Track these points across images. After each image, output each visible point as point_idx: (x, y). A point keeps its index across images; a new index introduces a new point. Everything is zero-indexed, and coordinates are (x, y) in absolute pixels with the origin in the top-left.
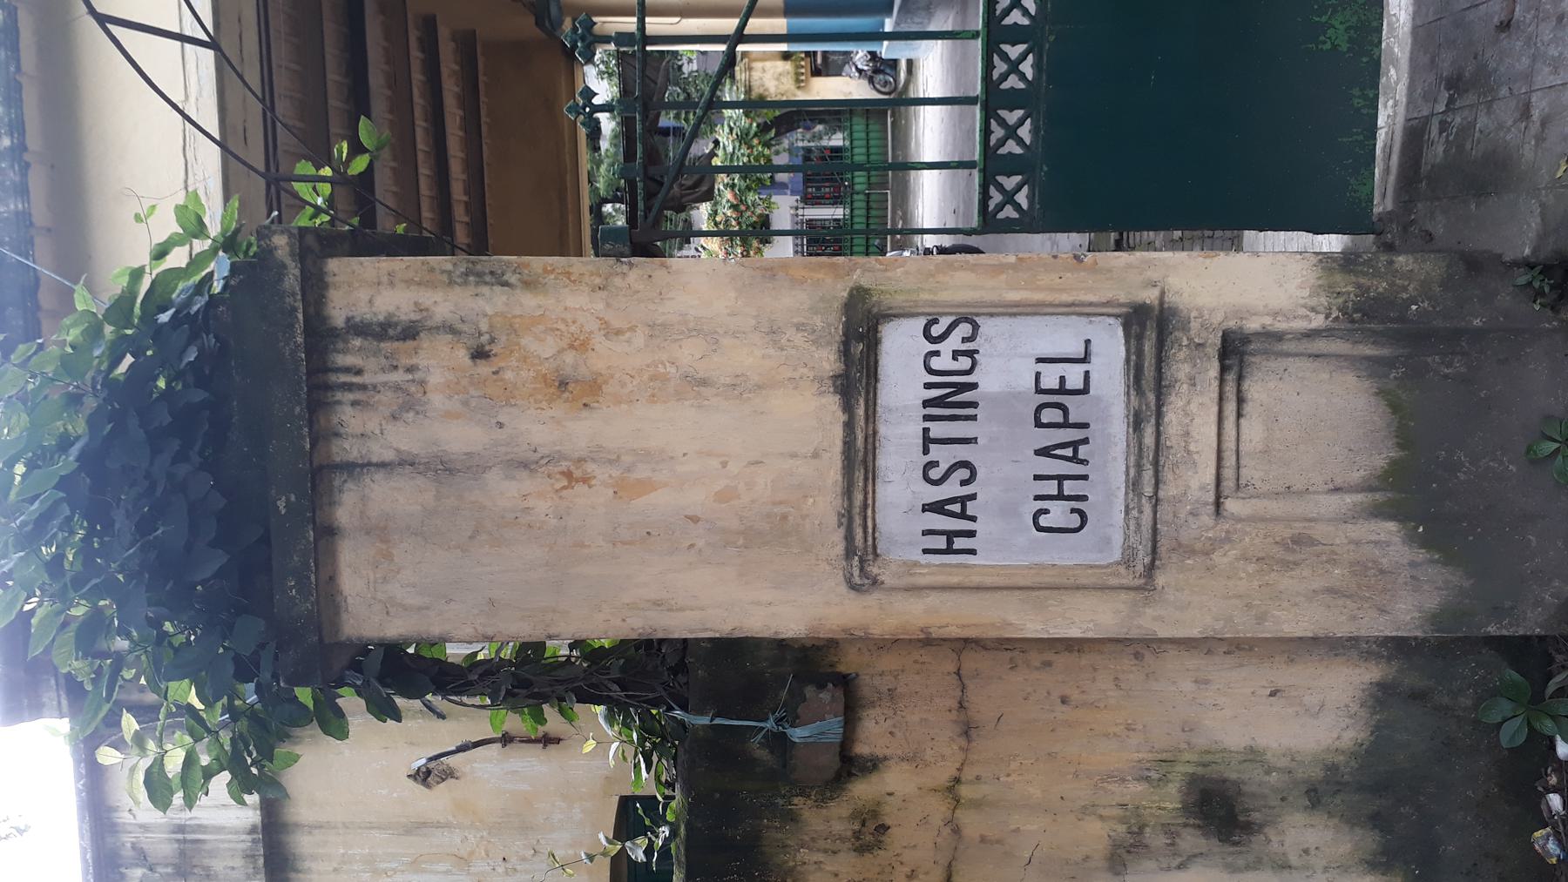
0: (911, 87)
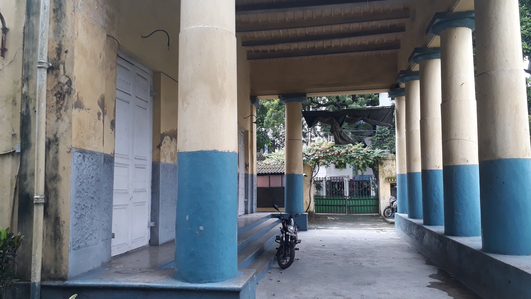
0: (386, 224)
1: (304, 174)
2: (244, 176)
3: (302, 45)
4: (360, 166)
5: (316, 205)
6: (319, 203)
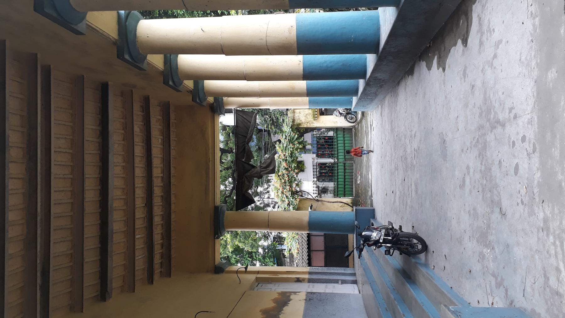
1: (309, 210)
2: (311, 284)
3: (158, 211)
5: (344, 196)
6: (342, 192)
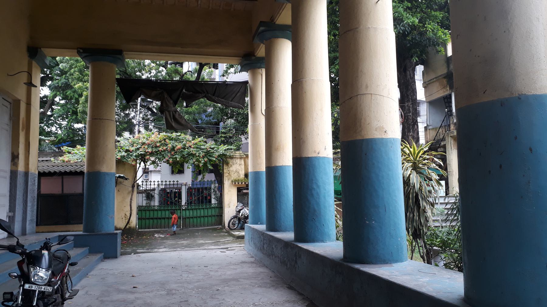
0: (231, 238)
1: (117, 175)
4: (201, 165)
5: (139, 219)
6: (144, 216)
